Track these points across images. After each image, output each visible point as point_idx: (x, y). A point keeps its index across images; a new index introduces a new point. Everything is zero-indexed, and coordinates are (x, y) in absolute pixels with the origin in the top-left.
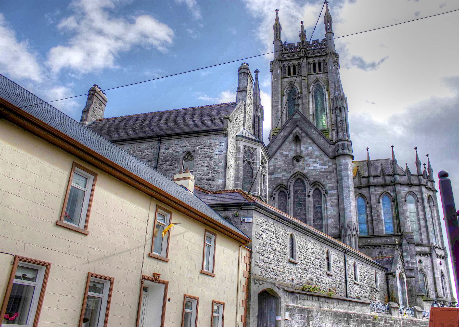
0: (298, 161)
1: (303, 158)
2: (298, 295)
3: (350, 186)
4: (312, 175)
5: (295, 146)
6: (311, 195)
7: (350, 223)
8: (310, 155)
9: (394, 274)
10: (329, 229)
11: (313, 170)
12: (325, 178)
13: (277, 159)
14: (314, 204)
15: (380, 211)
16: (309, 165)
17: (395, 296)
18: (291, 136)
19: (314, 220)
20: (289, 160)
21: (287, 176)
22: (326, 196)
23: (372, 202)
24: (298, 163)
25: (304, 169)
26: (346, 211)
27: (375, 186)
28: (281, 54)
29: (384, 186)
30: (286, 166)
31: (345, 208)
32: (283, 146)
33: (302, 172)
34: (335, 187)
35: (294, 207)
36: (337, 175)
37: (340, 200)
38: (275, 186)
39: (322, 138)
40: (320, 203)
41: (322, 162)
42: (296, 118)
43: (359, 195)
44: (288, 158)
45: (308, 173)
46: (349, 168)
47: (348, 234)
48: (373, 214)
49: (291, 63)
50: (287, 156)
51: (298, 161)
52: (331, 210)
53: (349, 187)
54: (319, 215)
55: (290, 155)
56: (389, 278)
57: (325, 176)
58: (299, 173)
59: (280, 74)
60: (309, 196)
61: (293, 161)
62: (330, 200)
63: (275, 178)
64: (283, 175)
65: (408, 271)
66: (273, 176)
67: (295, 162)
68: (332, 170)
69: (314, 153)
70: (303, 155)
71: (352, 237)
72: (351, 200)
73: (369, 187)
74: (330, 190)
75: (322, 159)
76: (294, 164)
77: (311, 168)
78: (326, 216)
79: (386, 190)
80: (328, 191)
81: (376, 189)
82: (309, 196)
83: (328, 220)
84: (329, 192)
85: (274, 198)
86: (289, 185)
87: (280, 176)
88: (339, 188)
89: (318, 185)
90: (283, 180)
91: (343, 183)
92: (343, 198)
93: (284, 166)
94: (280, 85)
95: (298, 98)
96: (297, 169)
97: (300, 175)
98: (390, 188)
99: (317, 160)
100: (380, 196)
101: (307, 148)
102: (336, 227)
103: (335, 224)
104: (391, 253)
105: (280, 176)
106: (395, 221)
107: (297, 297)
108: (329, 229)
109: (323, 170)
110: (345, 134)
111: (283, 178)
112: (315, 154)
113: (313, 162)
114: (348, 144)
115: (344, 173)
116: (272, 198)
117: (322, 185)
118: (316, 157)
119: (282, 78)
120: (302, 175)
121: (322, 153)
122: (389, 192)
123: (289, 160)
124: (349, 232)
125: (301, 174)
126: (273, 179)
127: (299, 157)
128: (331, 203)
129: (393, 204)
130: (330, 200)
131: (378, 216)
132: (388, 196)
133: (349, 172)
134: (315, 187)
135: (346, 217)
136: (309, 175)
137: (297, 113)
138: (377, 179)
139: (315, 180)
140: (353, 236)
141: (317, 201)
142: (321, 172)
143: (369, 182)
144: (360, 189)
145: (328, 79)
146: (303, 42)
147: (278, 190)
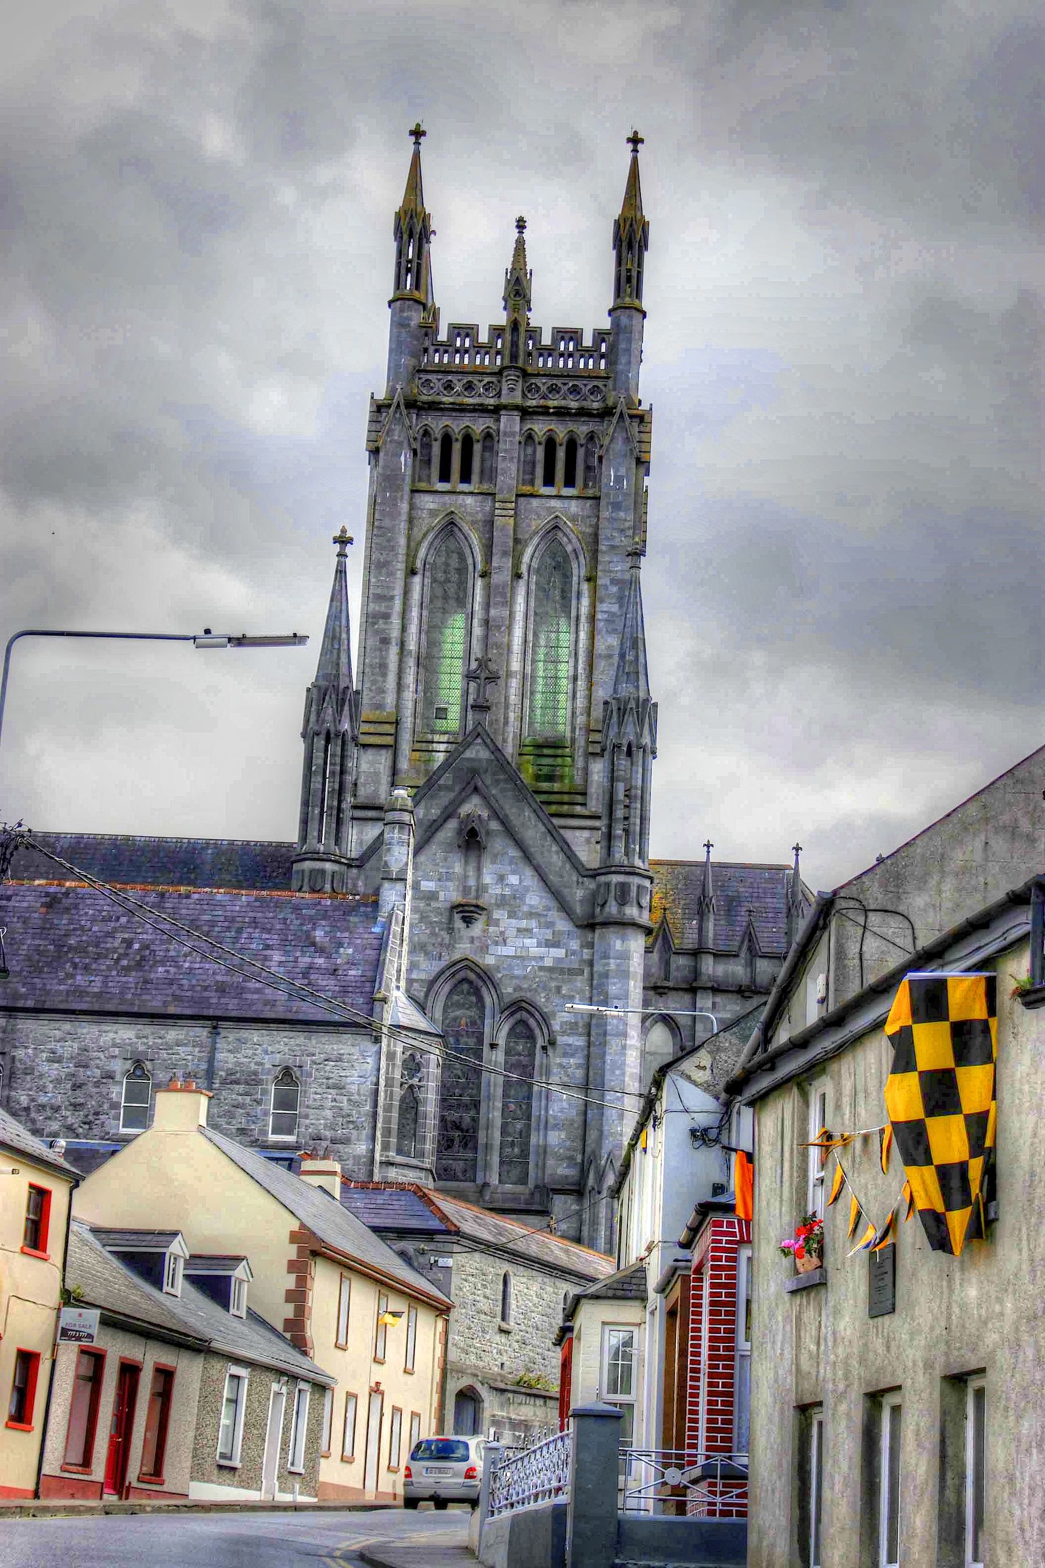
2: (510, 1395)
4: (513, 977)
6: (501, 1041)
10: (550, 1162)
30: (428, 931)
33: (480, 961)
34: (580, 1025)
36: (591, 986)
37: (591, 1074)
45: (498, 969)
46: (631, 969)
52: (561, 1100)
53: (625, 1035)
57: (553, 984)
60: (493, 1046)
62: (561, 1065)
74: (564, 1033)
78: (543, 1118)
80: (559, 1038)
82: (493, 1046)
83: (549, 1132)
84: (561, 1040)
88: (593, 1033)
97: (472, 970)
107: (509, 1399)
109: (548, 963)
115: (614, 984)
120: (478, 971)
133: (632, 983)
134: (518, 1016)
136: (500, 975)
139: (517, 995)
142: (541, 968)
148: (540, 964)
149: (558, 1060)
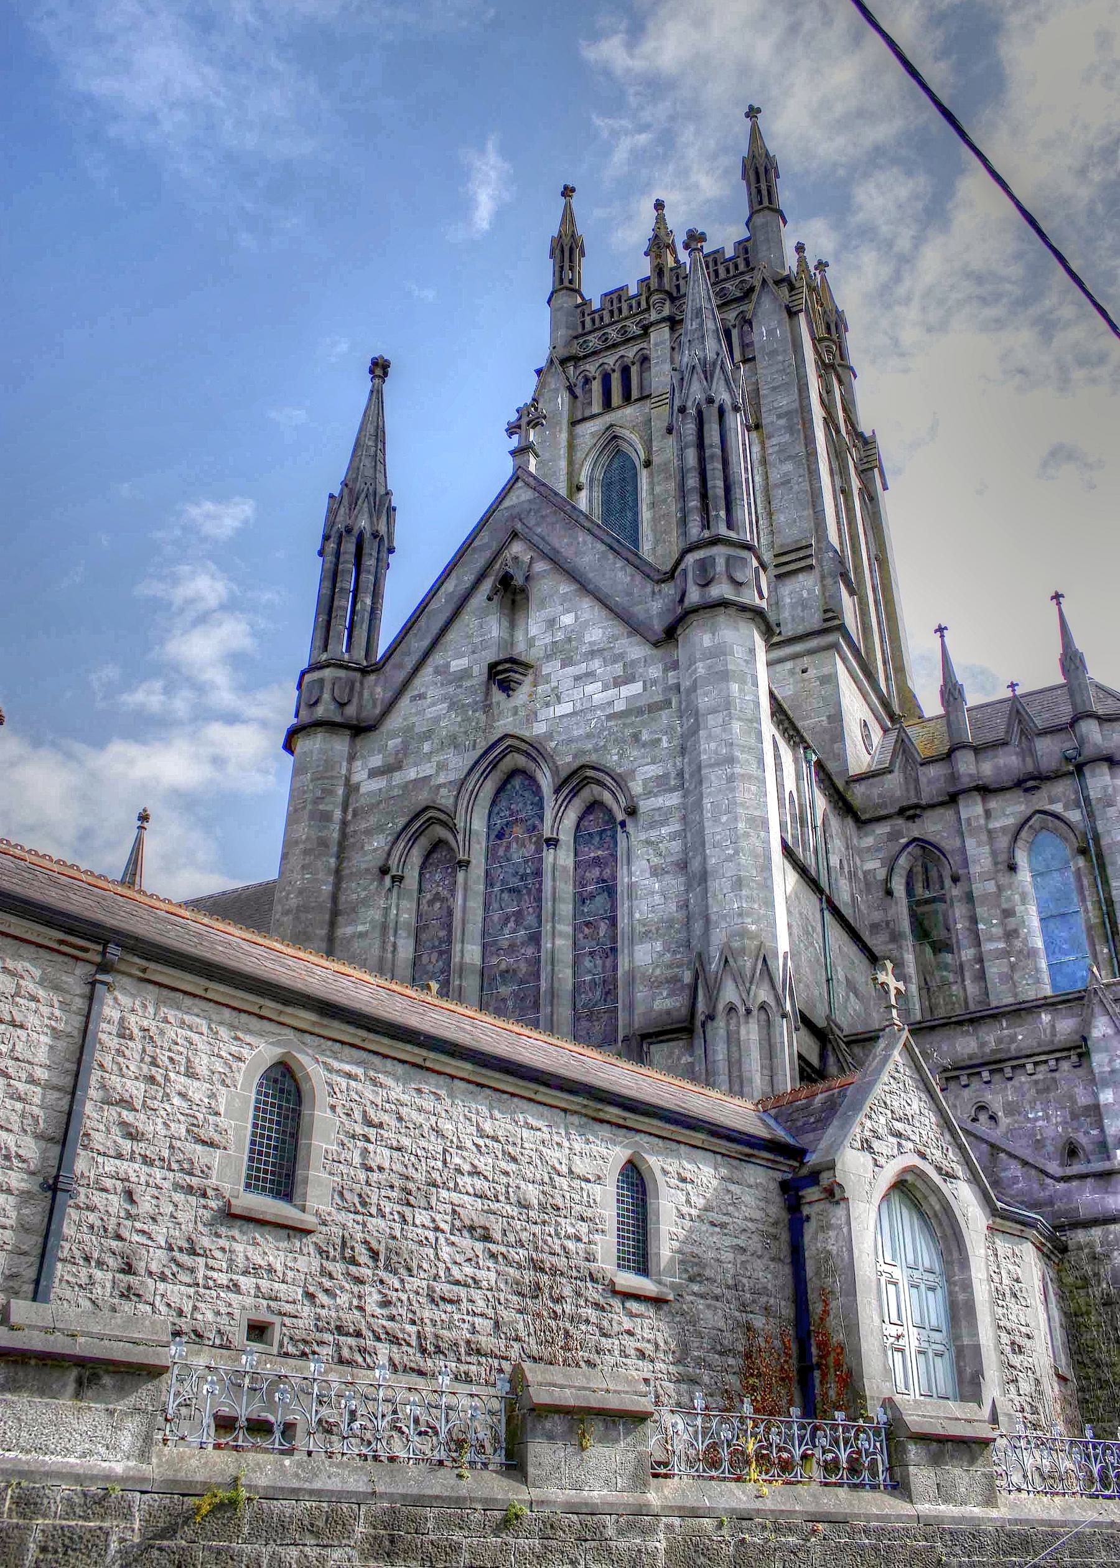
0: (507, 687)
1: (531, 671)
3: (737, 754)
5: (506, 624)
7: (736, 945)
8: (565, 652)
9: (825, 1179)
11: (574, 714)
12: (629, 739)
13: (421, 696)
14: (580, 882)
15: (1019, 909)
16: (558, 698)
17: (839, 1337)
18: (487, 586)
19: (576, 962)
20: (476, 693)
21: (458, 763)
22: (630, 827)
23: (975, 869)
24: (509, 696)
25: (531, 718)
26: (714, 885)
27: (985, 790)
28: (576, 337)
29: (1030, 784)
30: (459, 719)
31: (709, 868)
32: (452, 636)
33: (525, 733)
34: (673, 775)
35: (487, 906)
38: (401, 822)
39: (620, 564)
40: (607, 872)
41: (618, 669)
42: (513, 506)
43: (909, 849)
44: (467, 684)
45: (549, 736)
47: (721, 1007)
48: (981, 926)
49: (610, 360)
50: (465, 674)
51: (507, 687)
54: (603, 928)
55: (476, 670)
56: (806, 1211)
57: (628, 732)
58: (508, 744)
59: (566, 408)
61: (488, 693)
62: (648, 843)
63: (405, 786)
64: (441, 767)
65: (1090, 1181)
66: (398, 778)
67: (497, 695)
68: (659, 698)
69: (580, 638)
70: (532, 655)
71: (742, 1020)
72: (741, 825)
73: (952, 799)
74: (649, 794)
75: (618, 658)
76: (490, 706)
77: (565, 708)
79: (1041, 800)
80: (641, 803)
81: (993, 804)
82: (553, 842)
83: (636, 948)
85: (398, 879)
86: (461, 811)
87: (428, 769)
89: (599, 783)
90: (440, 786)
91: (704, 746)
92: (701, 823)
93: (450, 723)
94: (563, 452)
95: (528, 423)
96: (506, 724)
97: (518, 750)
98: (1063, 788)
99: (596, 664)
100: (1015, 838)
101: (551, 623)
102: (675, 980)
103: (670, 966)
104: (1038, 1106)
105: (428, 772)
106: (1098, 948)
108: (639, 996)
109: (619, 706)
110: (717, 516)
111: (441, 779)
112: (587, 639)
113: (577, 678)
114: (729, 559)
115: (706, 695)
116: (388, 880)
117: (613, 779)
118: (592, 654)
119: (574, 423)
120: (524, 746)
121: (619, 629)
122: (1058, 808)
123: (472, 690)
124: (729, 993)
125: (516, 743)
126: (396, 792)
127: (508, 665)
128: (656, 860)
129: (1081, 862)
130: (648, 843)
131: (1011, 935)
132: (1054, 831)
134: (586, 794)
135: (714, 918)
136: (553, 744)
137: (520, 484)
138: (996, 757)
140: (748, 1012)
141: (597, 862)
143: (953, 777)
144: (912, 818)
145: (757, 383)
146: (659, 271)
147: (415, 838)
148: (609, 711)
149: (643, 836)
